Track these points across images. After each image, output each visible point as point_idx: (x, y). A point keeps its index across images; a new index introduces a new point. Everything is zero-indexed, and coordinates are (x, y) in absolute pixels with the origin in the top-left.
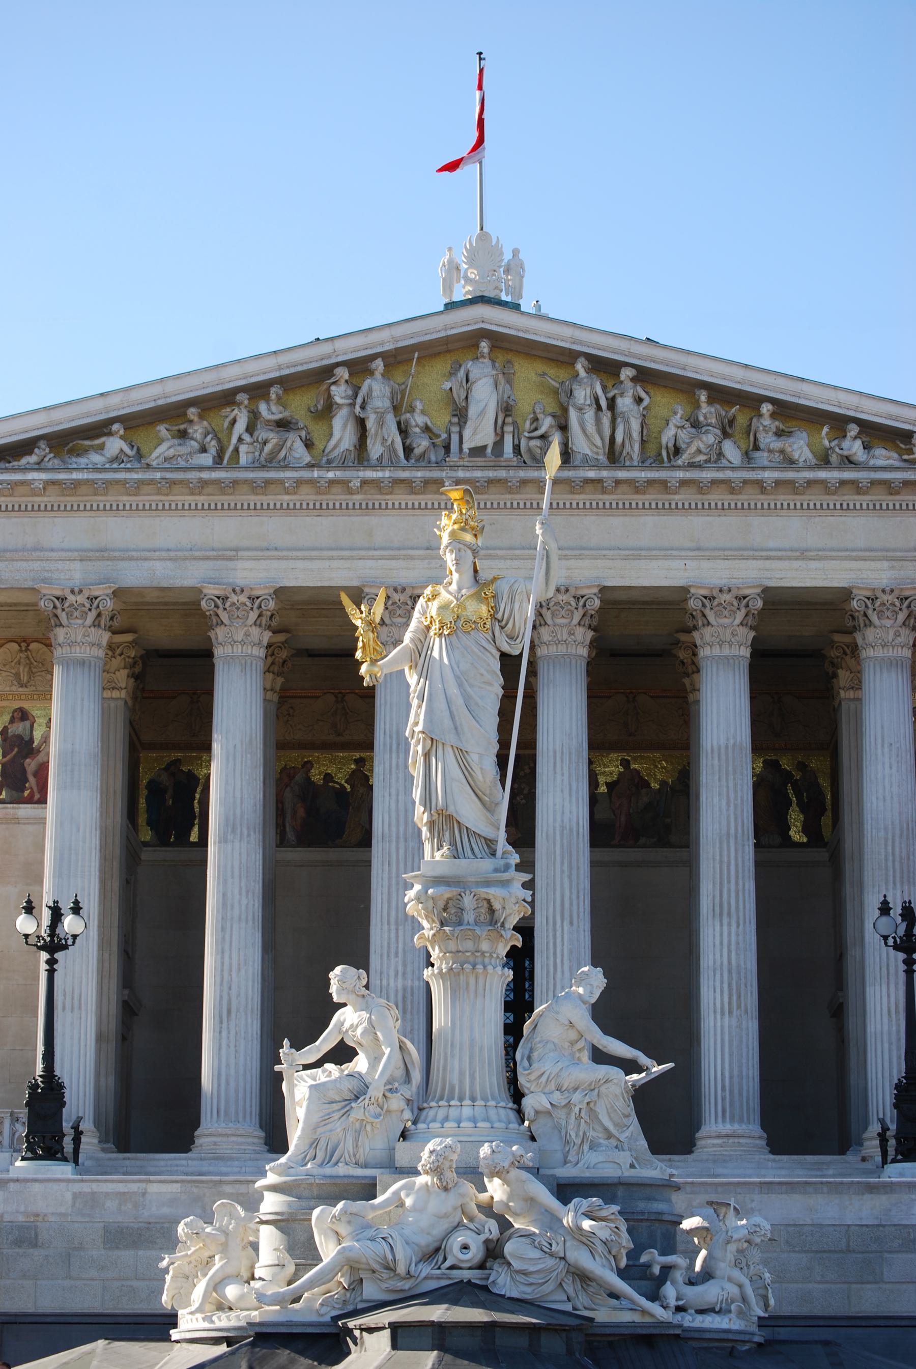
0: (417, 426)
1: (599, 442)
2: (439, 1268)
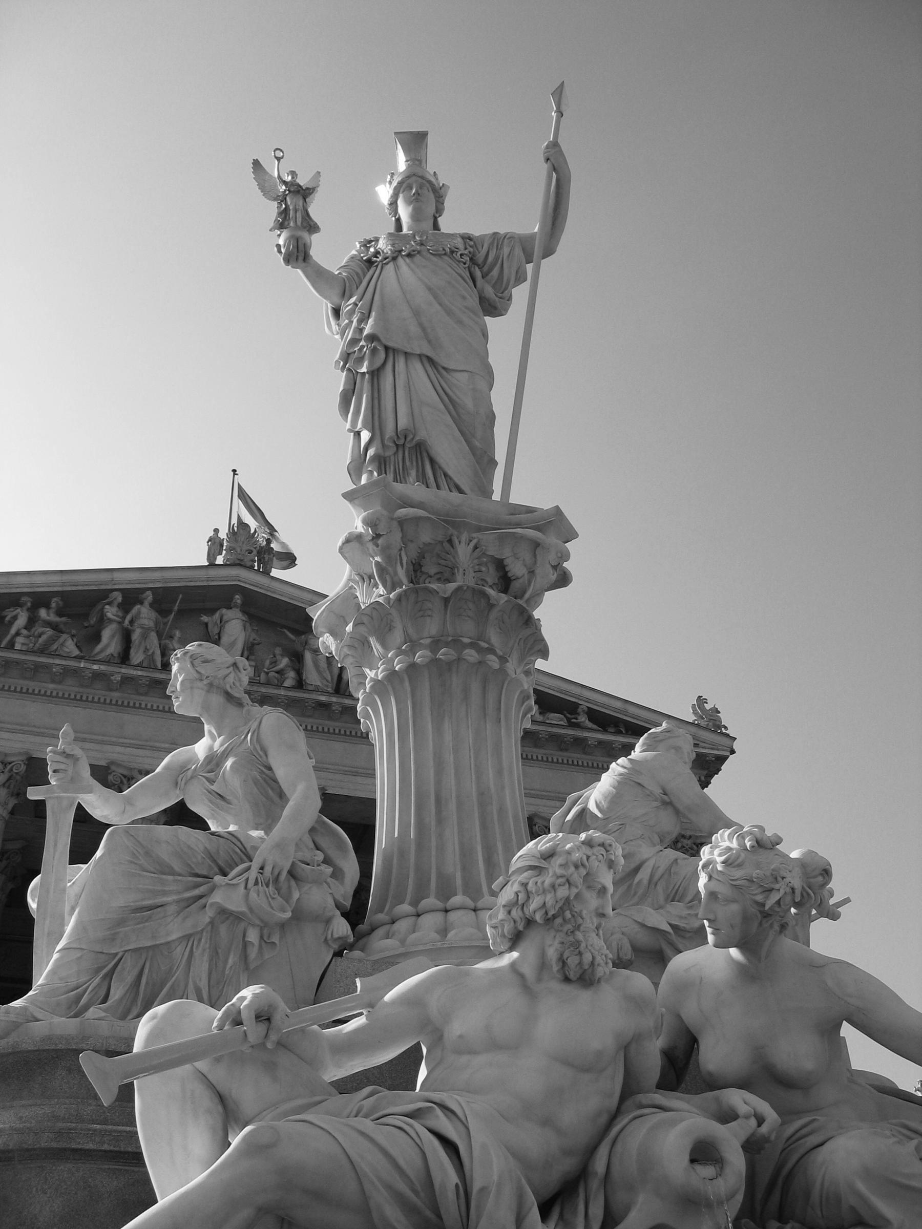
1: (329, 678)
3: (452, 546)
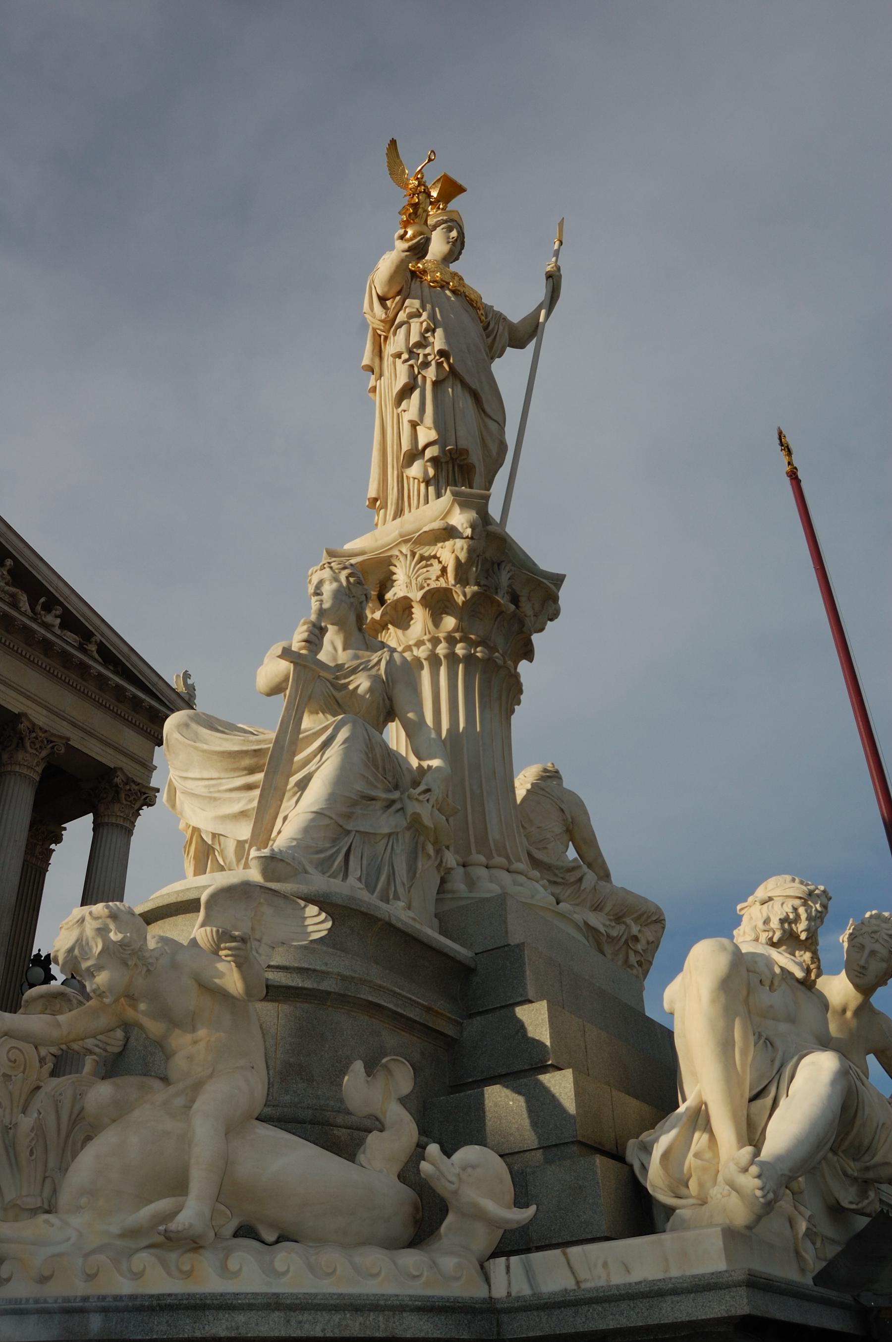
3: (499, 569)
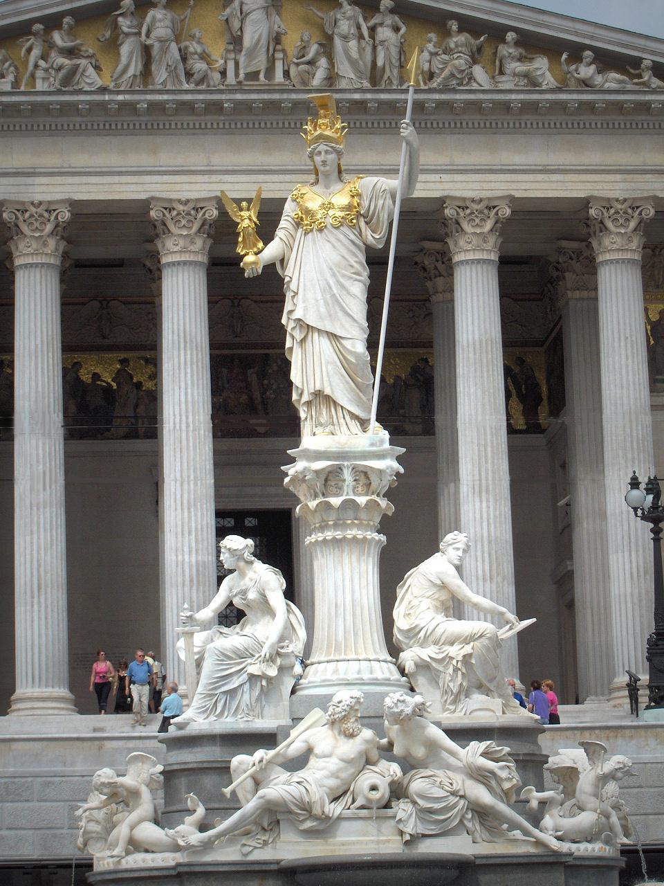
0: (196, 53)
2: (349, 809)
